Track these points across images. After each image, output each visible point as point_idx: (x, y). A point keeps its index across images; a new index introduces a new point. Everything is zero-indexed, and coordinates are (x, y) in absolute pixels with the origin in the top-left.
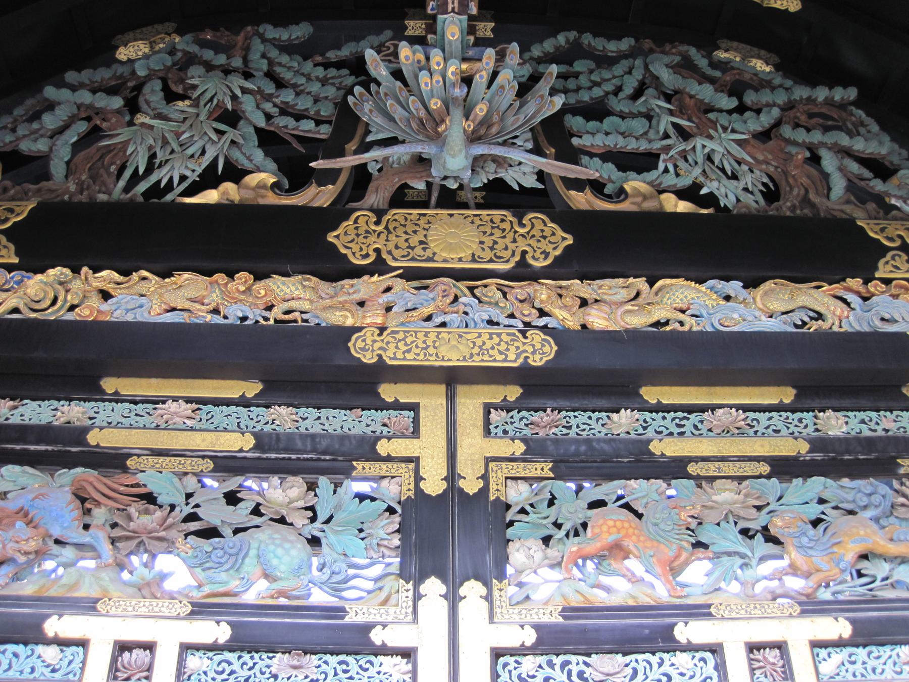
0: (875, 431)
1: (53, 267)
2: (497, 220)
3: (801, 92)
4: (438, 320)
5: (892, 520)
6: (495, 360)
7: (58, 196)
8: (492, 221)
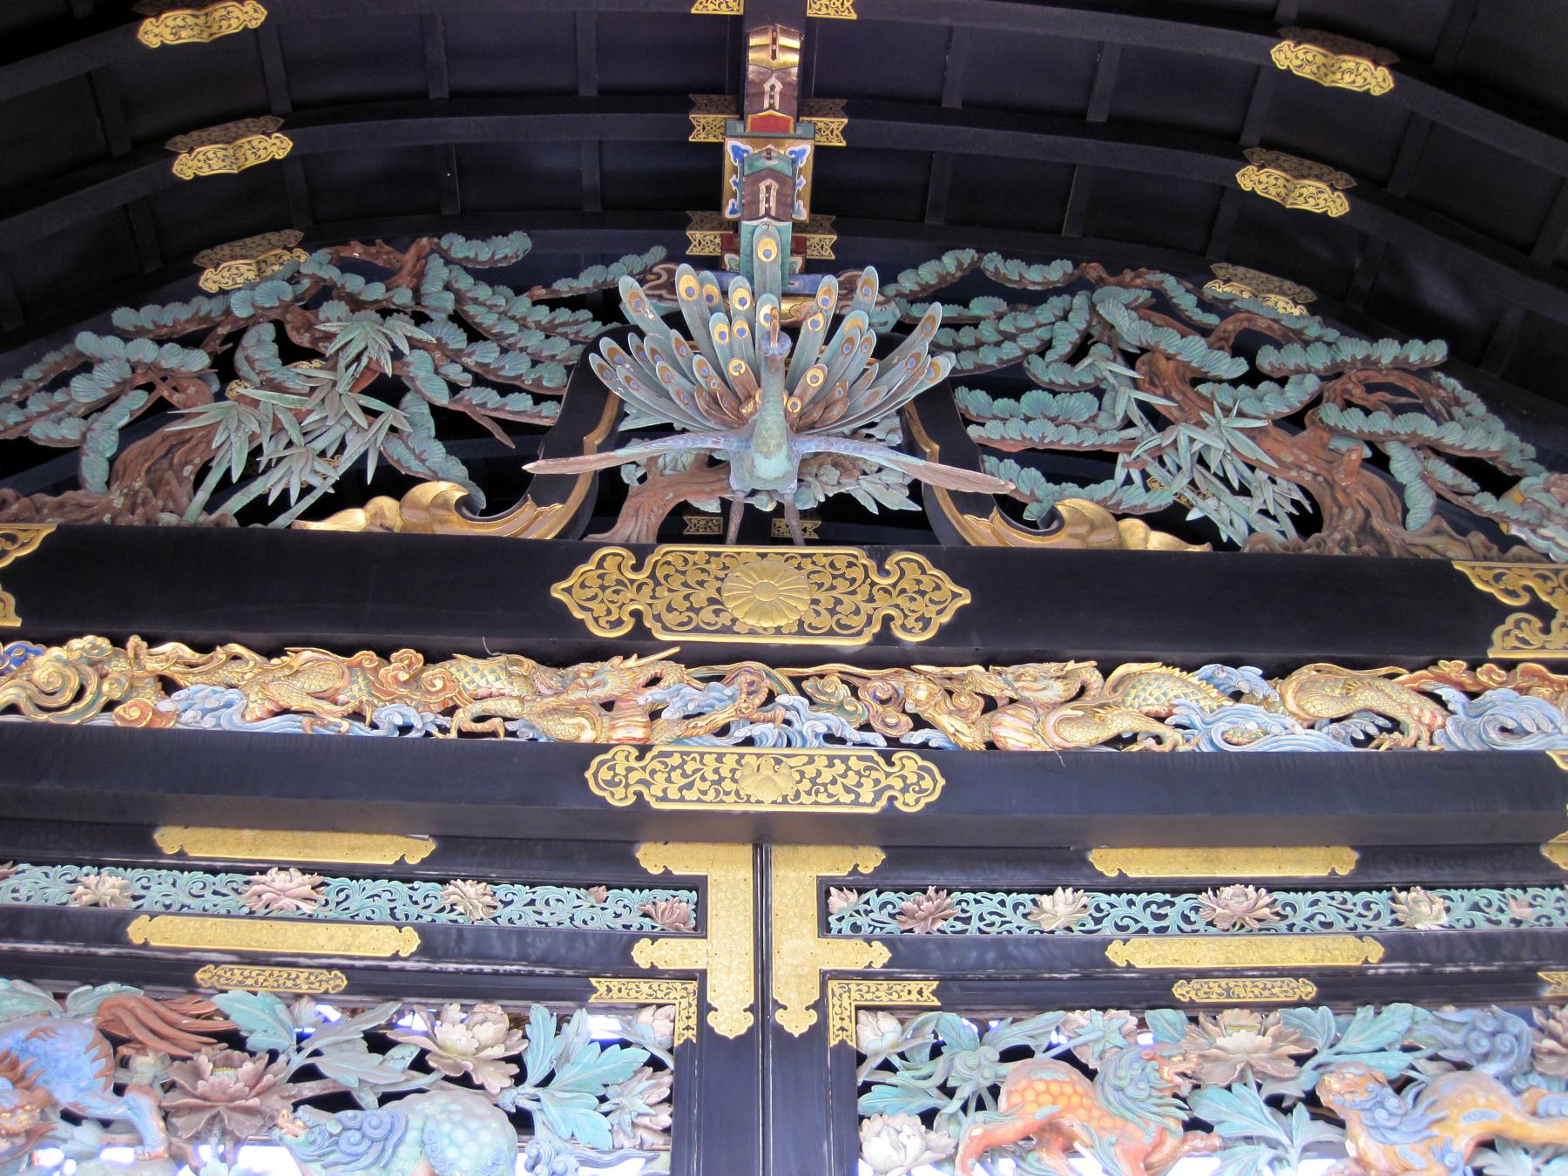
0: (1498, 923)
1: (80, 635)
2: (841, 564)
3: (1353, 349)
4: (740, 733)
5: (1534, 1079)
6: (837, 803)
7: (92, 516)
8: (832, 565)
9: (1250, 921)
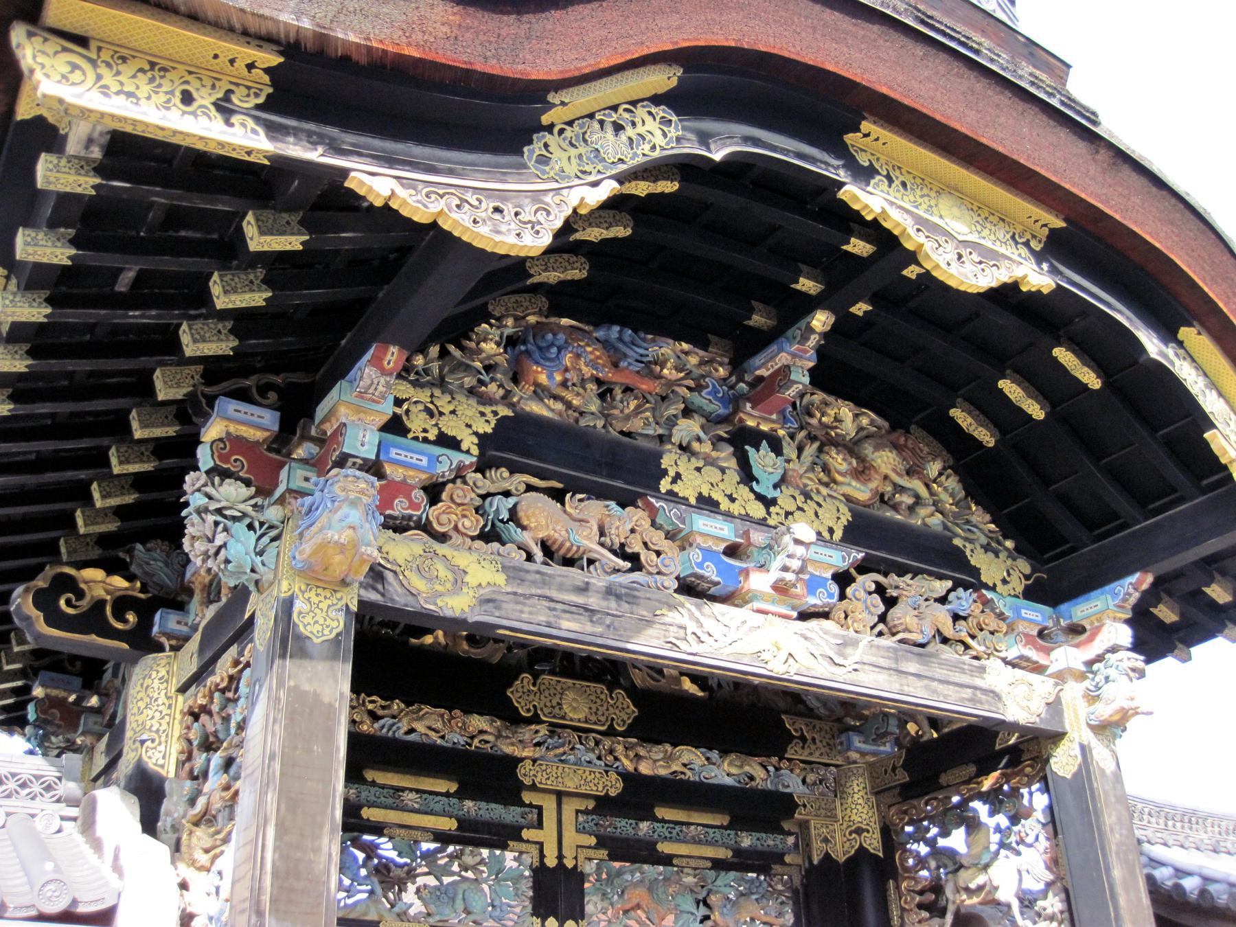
9: (694, 837)
